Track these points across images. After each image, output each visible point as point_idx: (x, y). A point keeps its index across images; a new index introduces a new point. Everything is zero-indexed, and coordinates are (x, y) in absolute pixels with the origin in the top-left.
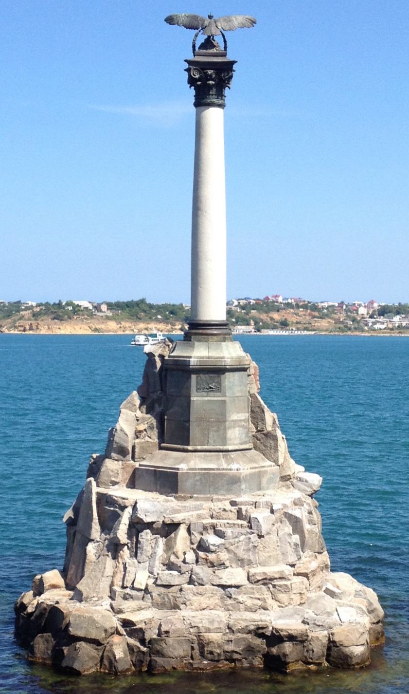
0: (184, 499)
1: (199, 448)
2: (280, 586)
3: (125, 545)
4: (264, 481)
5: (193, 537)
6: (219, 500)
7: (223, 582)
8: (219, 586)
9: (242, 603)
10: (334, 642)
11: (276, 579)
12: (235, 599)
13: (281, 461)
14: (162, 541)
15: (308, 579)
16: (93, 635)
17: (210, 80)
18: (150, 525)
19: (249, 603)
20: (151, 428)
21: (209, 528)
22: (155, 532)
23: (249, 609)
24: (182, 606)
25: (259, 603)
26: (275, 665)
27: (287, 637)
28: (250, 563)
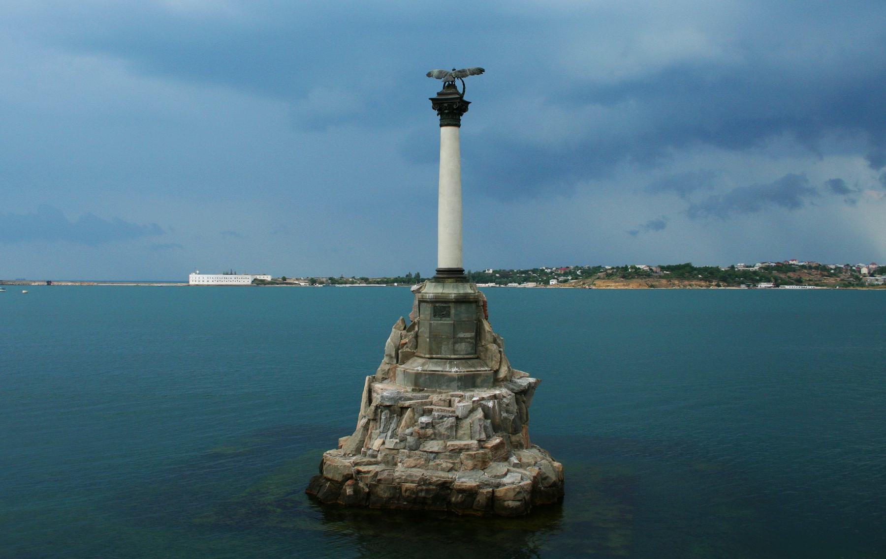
4: (479, 381)
6: (440, 393)
17: (451, 108)
19: (444, 465)
20: (410, 341)
23: (443, 470)
24: (399, 464)
25: (452, 466)
28: (448, 438)
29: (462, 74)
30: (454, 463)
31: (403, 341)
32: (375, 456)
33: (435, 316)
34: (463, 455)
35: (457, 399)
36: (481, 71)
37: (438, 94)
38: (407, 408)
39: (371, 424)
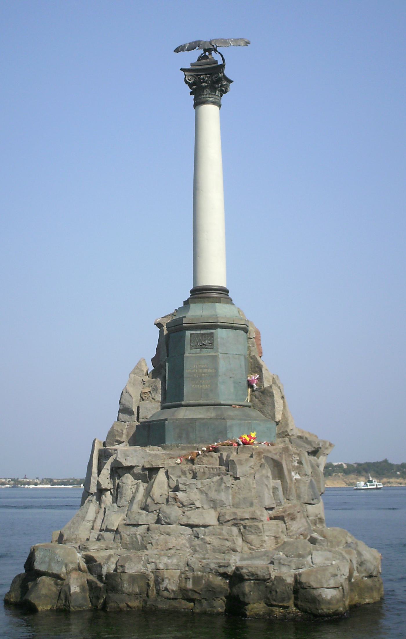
0: (170, 448)
1: (192, 402)
2: (250, 527)
3: (106, 490)
5: (171, 481)
7: (191, 522)
8: (186, 525)
9: (209, 544)
10: (300, 583)
11: (248, 519)
12: (202, 539)
13: (279, 417)
14: (142, 487)
15: (285, 523)
16: (55, 569)
18: (129, 469)
21: (188, 473)
22: (136, 477)
24: (149, 546)
26: (236, 606)
27: (247, 575)
37: (192, 65)
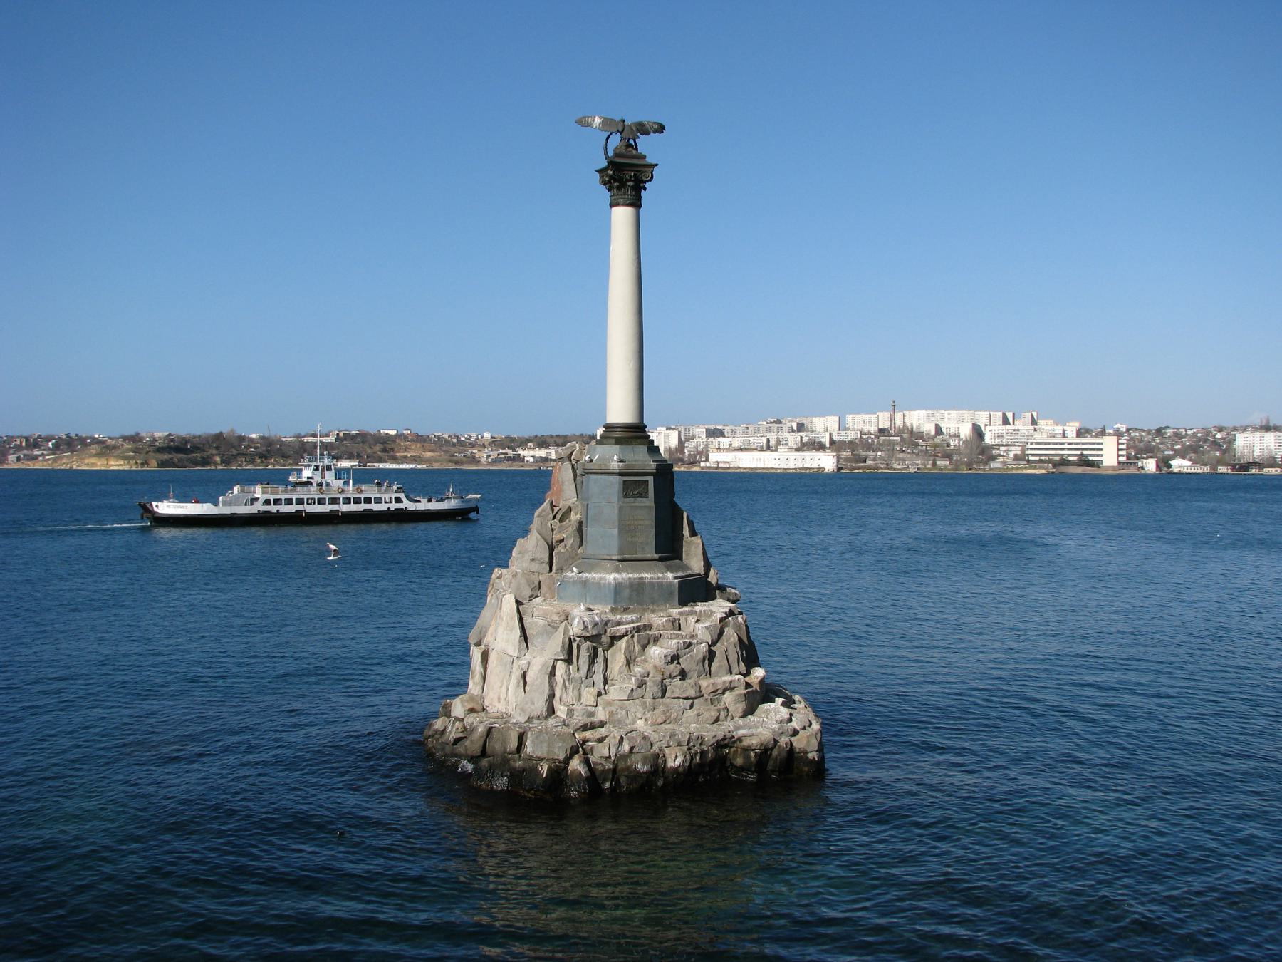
6: (653, 611)
29: (642, 129)
30: (719, 711)
31: (557, 537)
32: (592, 714)
33: (625, 496)
34: (728, 698)
35: (692, 620)
36: (661, 129)
38: (621, 637)
39: (561, 667)
